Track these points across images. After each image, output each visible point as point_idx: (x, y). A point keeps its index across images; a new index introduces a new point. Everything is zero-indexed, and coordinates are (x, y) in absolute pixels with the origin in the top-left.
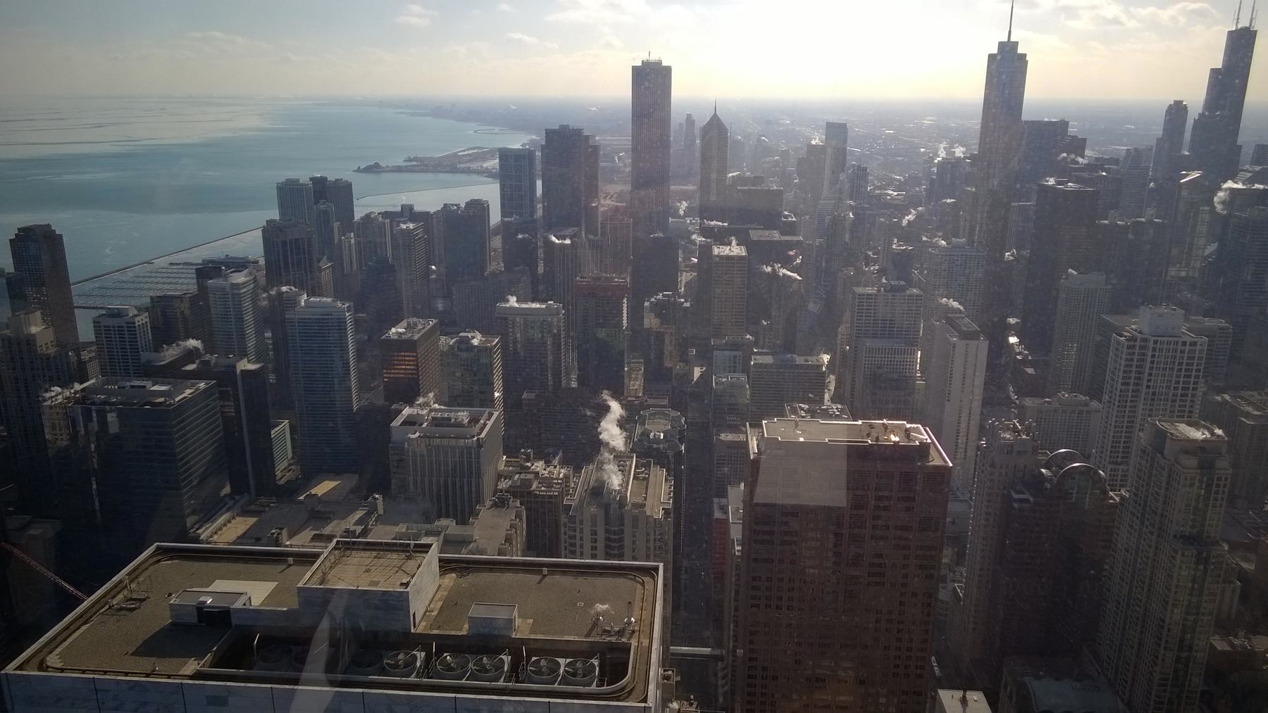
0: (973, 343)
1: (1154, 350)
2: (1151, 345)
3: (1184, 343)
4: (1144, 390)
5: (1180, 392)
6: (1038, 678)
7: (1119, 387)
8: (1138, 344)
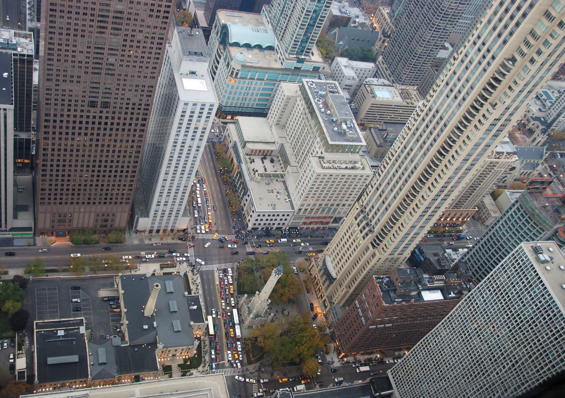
6: (234, 23)
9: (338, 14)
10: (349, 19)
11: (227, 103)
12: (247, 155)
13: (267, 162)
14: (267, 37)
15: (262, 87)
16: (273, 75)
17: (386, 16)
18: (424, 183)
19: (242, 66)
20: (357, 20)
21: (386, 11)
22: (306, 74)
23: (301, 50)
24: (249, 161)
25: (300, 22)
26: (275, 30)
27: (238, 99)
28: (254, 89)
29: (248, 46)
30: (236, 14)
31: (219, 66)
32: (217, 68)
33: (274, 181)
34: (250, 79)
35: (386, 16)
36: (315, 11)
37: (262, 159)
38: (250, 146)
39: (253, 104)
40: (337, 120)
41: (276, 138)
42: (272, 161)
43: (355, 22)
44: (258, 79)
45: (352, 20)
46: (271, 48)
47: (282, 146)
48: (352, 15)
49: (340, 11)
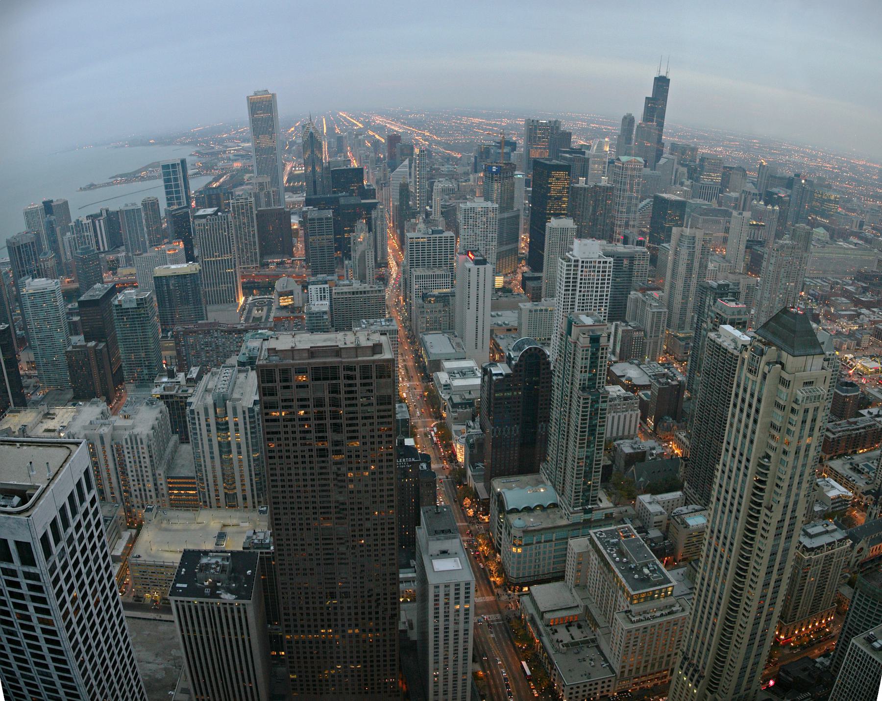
0: (481, 267)
1: (582, 267)
2: (580, 264)
3: (600, 262)
4: (578, 293)
5: (599, 294)
6: (510, 489)
7: (563, 292)
8: (573, 263)
9: (631, 451)
10: (644, 453)
11: (518, 574)
12: (548, 626)
13: (574, 630)
14: (544, 493)
15: (553, 549)
16: (562, 534)
17: (684, 439)
18: (736, 612)
19: (524, 532)
20: (654, 452)
21: (682, 435)
22: (598, 523)
23: (586, 499)
24: (551, 632)
25: (575, 472)
26: (554, 486)
27: (530, 567)
28: (545, 553)
29: (528, 509)
30: (512, 479)
31: (503, 537)
32: (501, 539)
33: (586, 649)
34: (545, 542)
35: (684, 439)
36: (587, 457)
37: (567, 627)
38: (547, 616)
39: (549, 569)
40: (636, 567)
41: (578, 601)
42: (579, 627)
43: (652, 454)
44: (545, 542)
45: (648, 453)
46: (555, 505)
47: (586, 608)
48: (647, 449)
49: (632, 448)
